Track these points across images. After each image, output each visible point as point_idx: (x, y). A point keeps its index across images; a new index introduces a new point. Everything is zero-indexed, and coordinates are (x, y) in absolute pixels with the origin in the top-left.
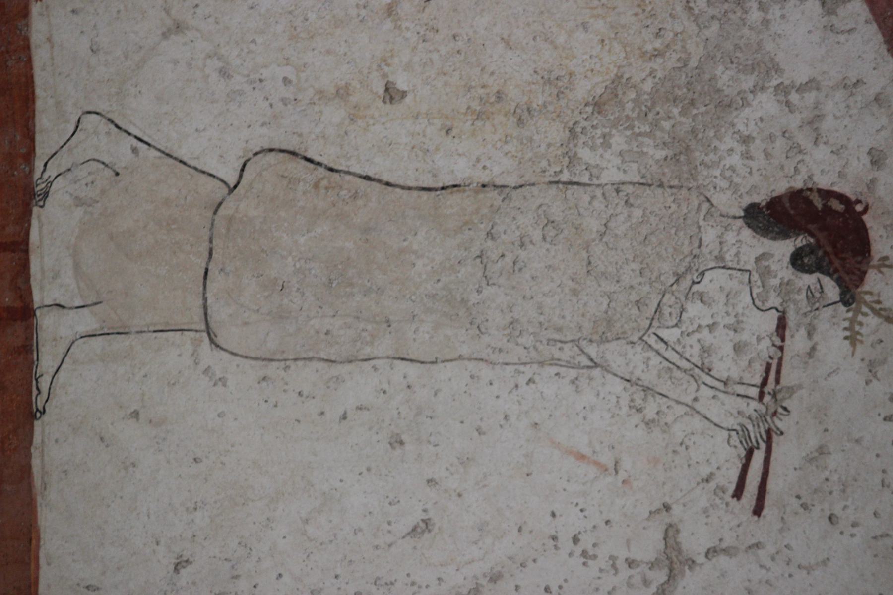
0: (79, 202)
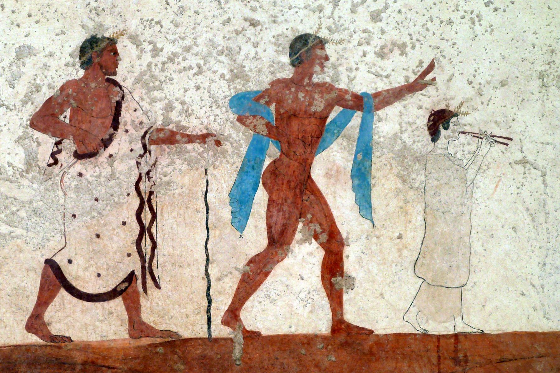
0: (427, 321)
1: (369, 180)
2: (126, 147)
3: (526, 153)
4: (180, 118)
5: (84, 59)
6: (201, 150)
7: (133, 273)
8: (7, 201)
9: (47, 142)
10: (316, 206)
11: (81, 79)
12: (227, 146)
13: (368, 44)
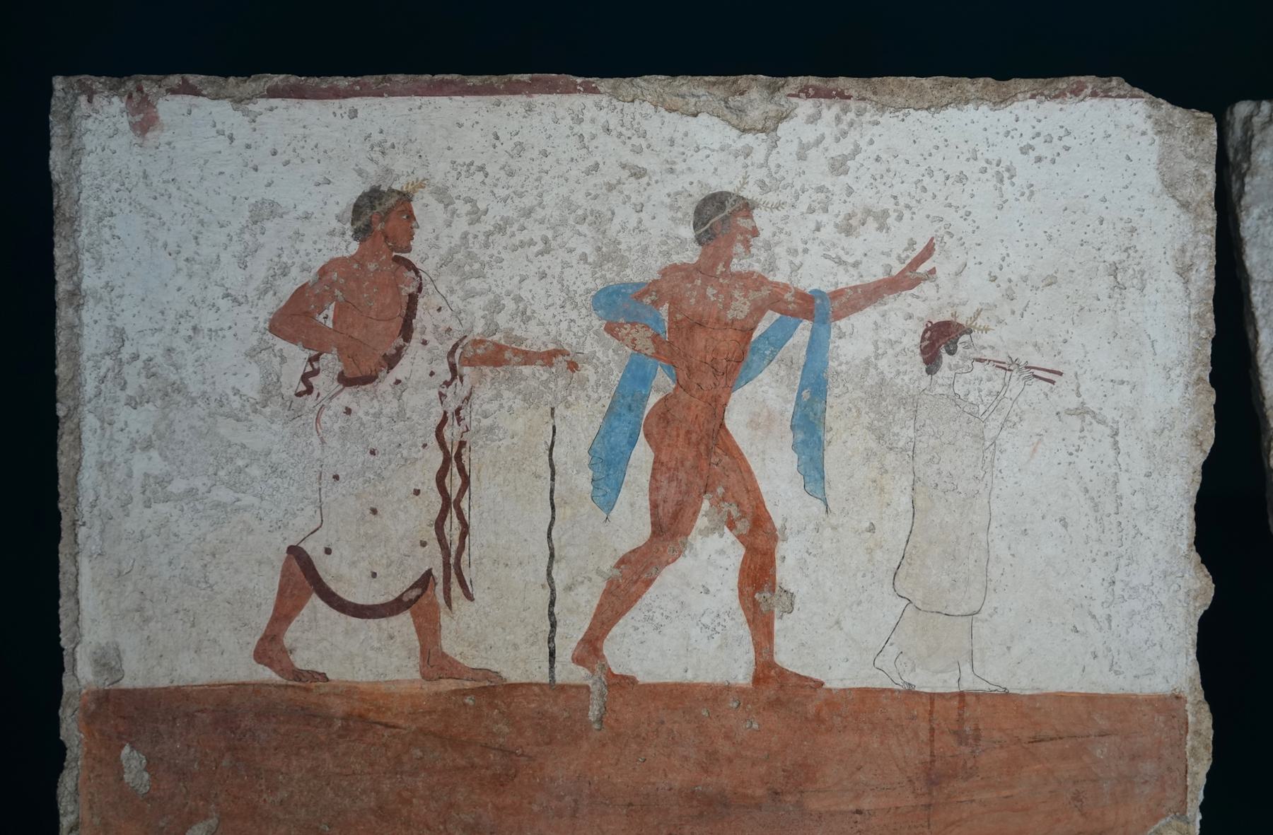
1: (821, 434)
2: (422, 370)
3: (1085, 397)
4: (511, 324)
5: (359, 224)
6: (545, 376)
7: (429, 573)
8: (229, 450)
9: (297, 357)
10: (732, 475)
11: (352, 257)
12: (588, 371)
13: (826, 210)
